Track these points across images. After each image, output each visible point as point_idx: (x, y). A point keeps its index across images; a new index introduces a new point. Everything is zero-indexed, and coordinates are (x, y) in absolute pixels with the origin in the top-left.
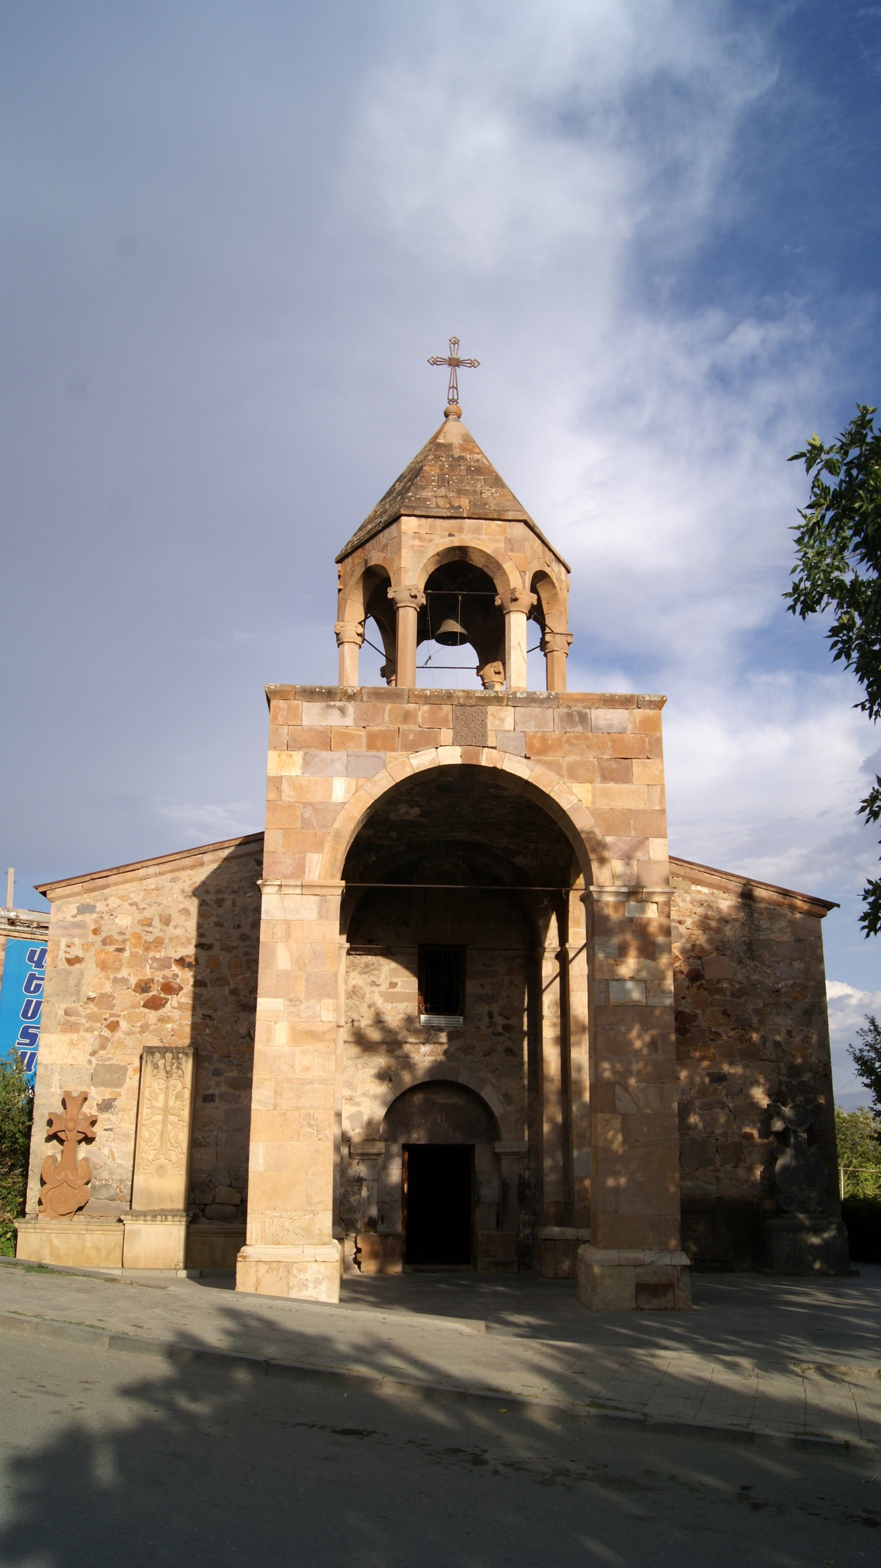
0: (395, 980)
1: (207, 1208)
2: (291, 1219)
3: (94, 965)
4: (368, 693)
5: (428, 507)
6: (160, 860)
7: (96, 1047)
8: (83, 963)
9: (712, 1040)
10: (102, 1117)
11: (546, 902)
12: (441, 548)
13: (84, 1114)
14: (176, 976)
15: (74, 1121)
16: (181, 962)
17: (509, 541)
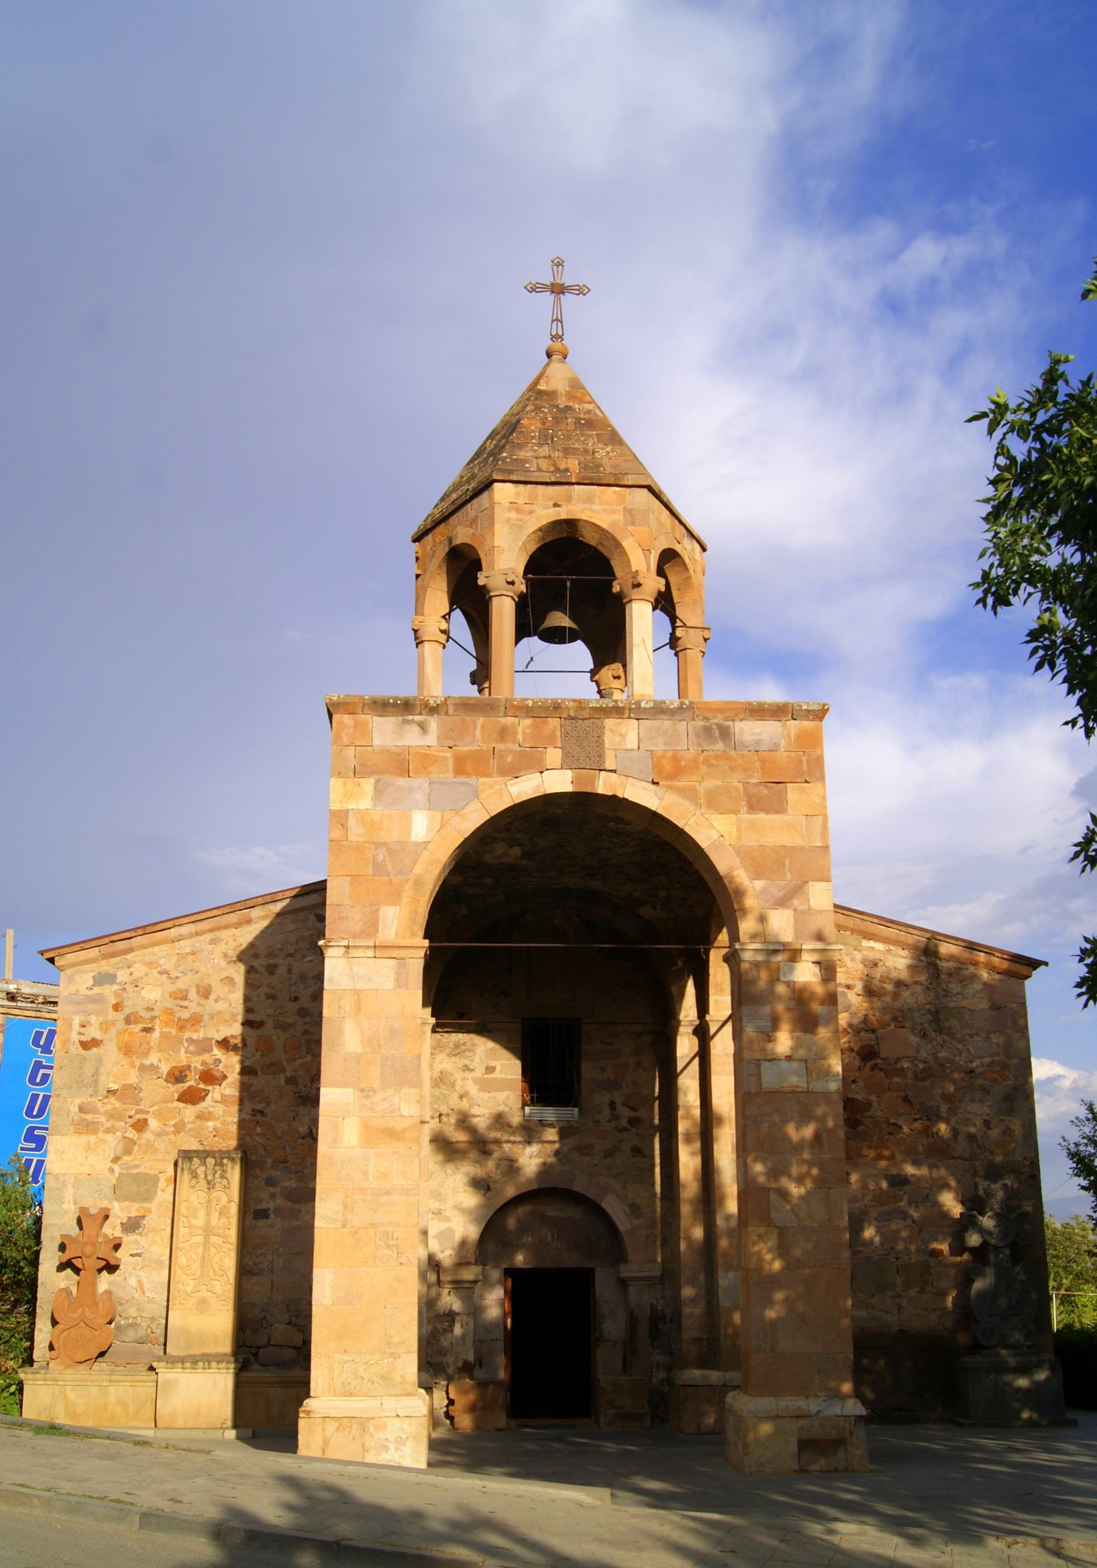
0: (492, 1063)
1: (261, 1350)
2: (366, 1363)
3: (115, 1049)
4: (455, 705)
5: (527, 471)
6: (197, 917)
7: (119, 1152)
8: (102, 1047)
9: (890, 1134)
10: (128, 1240)
11: (680, 964)
12: (544, 522)
13: (106, 1236)
14: (219, 1061)
15: (93, 1245)
16: (224, 1044)
17: (629, 512)
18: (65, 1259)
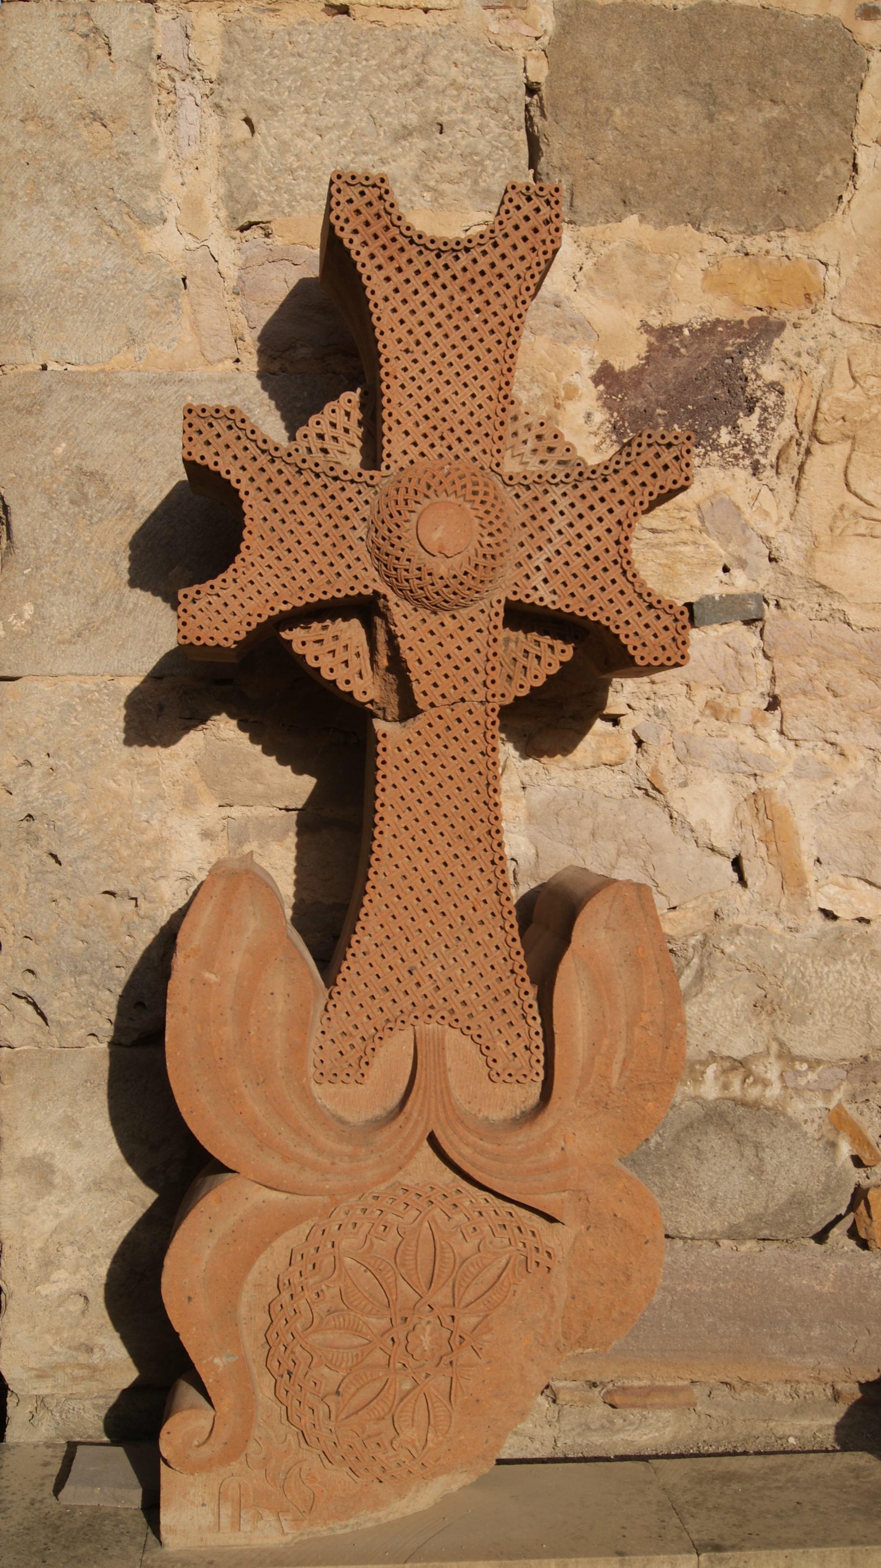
18: (227, 610)
